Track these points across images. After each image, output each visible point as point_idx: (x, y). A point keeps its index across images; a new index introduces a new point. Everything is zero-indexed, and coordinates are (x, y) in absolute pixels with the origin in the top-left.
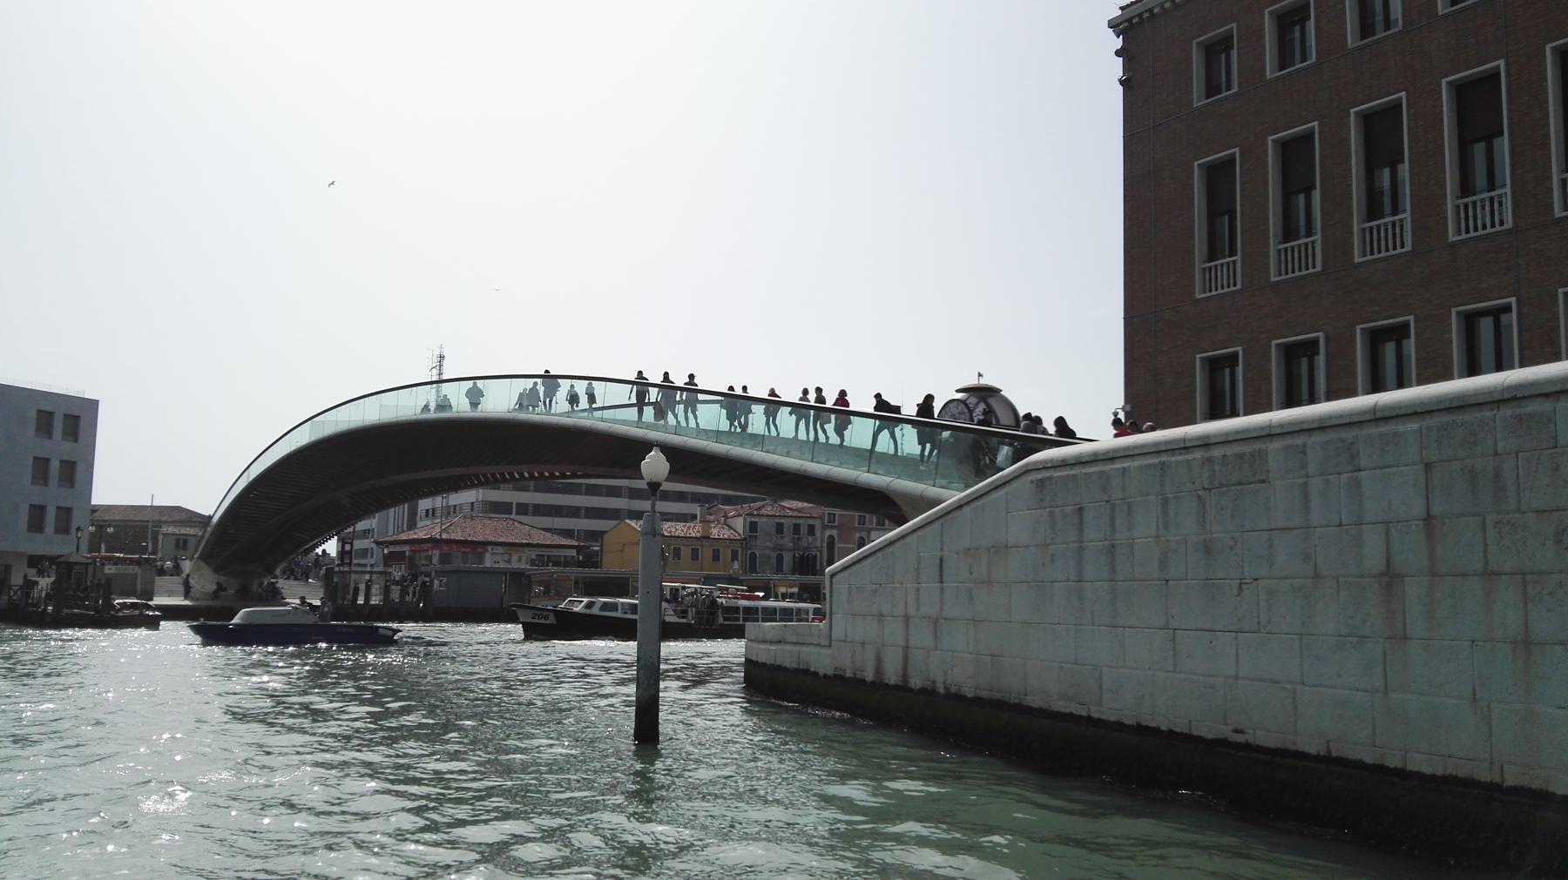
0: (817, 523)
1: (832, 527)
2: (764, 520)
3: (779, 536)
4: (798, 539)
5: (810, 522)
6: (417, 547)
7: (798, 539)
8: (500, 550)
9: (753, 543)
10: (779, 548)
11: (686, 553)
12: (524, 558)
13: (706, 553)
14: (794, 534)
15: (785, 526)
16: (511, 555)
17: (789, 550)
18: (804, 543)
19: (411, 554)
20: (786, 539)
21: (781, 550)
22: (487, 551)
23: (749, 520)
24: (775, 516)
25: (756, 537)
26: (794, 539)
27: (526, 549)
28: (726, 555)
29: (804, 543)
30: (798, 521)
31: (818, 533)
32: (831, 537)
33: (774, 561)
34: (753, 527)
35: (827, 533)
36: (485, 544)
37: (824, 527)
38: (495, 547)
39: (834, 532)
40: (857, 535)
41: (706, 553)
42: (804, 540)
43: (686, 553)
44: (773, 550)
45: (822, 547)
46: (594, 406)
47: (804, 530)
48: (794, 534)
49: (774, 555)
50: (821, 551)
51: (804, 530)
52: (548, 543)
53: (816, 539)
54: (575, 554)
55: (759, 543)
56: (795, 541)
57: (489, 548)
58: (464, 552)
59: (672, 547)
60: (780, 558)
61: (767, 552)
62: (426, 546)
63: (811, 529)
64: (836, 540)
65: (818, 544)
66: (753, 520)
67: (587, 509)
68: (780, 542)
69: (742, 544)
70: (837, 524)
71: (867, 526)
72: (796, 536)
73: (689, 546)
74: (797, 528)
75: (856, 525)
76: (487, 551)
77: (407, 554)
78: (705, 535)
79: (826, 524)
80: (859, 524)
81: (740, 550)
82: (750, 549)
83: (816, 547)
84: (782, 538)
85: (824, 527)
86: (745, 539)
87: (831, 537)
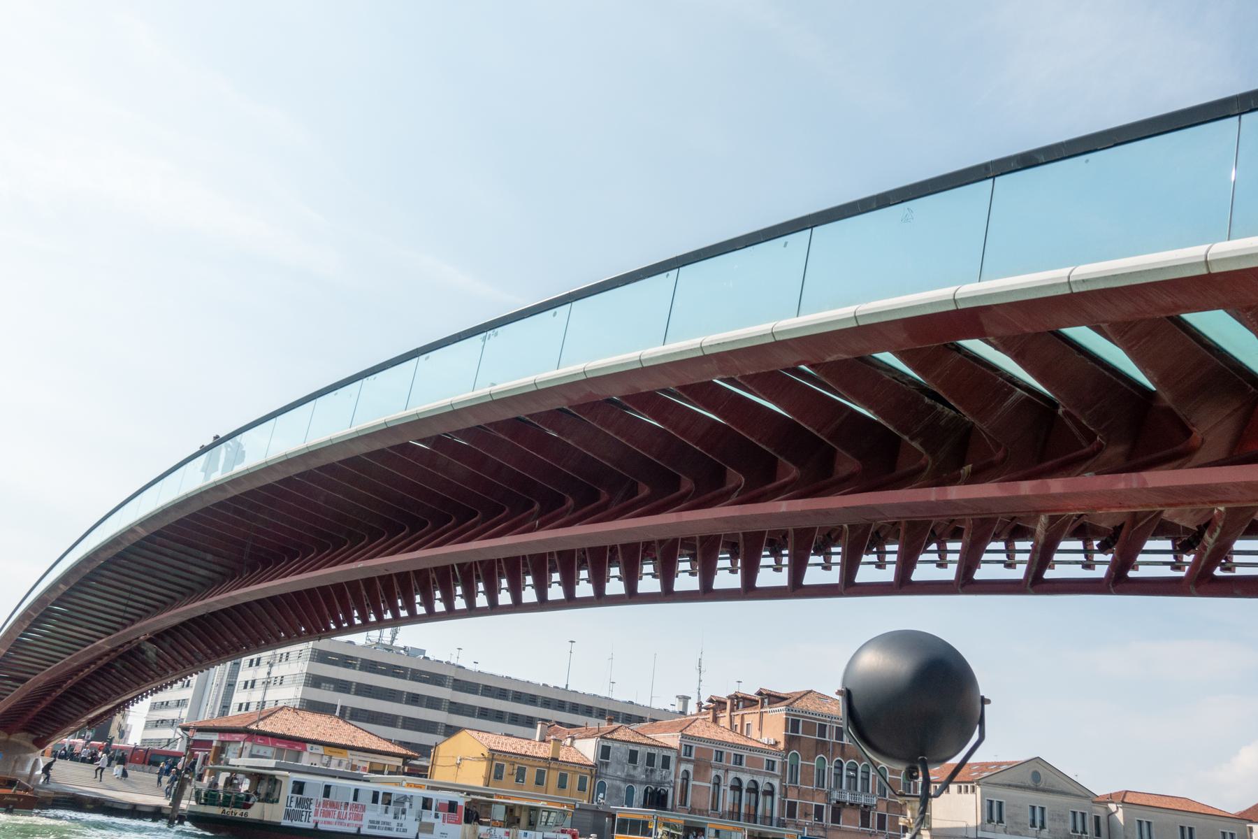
0: (673, 755)
1: (688, 761)
2: (617, 745)
3: (631, 766)
4: (652, 771)
5: (666, 753)
6: (226, 737)
8: (321, 750)
10: (630, 779)
11: (531, 774)
12: (344, 763)
13: (553, 778)
14: (647, 765)
17: (641, 783)
18: (657, 777)
19: (219, 745)
20: (639, 769)
21: (632, 782)
22: (306, 750)
23: (601, 743)
24: (629, 742)
25: (607, 764)
26: (647, 770)
27: (349, 752)
28: (573, 781)
29: (657, 777)
30: (653, 751)
31: (672, 766)
32: (687, 772)
33: (624, 795)
34: (605, 752)
35: (683, 767)
36: (304, 741)
37: (680, 760)
38: (315, 746)
39: (690, 767)
40: (714, 773)
41: (553, 778)
42: (658, 773)
43: (531, 774)
44: (625, 781)
47: (658, 762)
48: (647, 765)
49: (624, 786)
50: (674, 788)
52: (374, 748)
53: (670, 773)
54: (400, 764)
55: (610, 771)
56: (648, 773)
57: (309, 746)
58: (279, 749)
59: (516, 766)
60: (630, 791)
61: (618, 783)
62: (237, 737)
63: (666, 762)
64: (691, 777)
66: (605, 744)
67: (405, 719)
68: (632, 772)
69: (591, 770)
70: (693, 758)
71: (724, 763)
72: (650, 768)
73: (536, 767)
74: (651, 758)
76: (306, 750)
77: (214, 744)
78: (555, 757)
79: (682, 756)
80: (716, 760)
82: (600, 777)
83: (669, 783)
84: (635, 768)
85: (680, 760)
86: (595, 766)
87: (687, 772)
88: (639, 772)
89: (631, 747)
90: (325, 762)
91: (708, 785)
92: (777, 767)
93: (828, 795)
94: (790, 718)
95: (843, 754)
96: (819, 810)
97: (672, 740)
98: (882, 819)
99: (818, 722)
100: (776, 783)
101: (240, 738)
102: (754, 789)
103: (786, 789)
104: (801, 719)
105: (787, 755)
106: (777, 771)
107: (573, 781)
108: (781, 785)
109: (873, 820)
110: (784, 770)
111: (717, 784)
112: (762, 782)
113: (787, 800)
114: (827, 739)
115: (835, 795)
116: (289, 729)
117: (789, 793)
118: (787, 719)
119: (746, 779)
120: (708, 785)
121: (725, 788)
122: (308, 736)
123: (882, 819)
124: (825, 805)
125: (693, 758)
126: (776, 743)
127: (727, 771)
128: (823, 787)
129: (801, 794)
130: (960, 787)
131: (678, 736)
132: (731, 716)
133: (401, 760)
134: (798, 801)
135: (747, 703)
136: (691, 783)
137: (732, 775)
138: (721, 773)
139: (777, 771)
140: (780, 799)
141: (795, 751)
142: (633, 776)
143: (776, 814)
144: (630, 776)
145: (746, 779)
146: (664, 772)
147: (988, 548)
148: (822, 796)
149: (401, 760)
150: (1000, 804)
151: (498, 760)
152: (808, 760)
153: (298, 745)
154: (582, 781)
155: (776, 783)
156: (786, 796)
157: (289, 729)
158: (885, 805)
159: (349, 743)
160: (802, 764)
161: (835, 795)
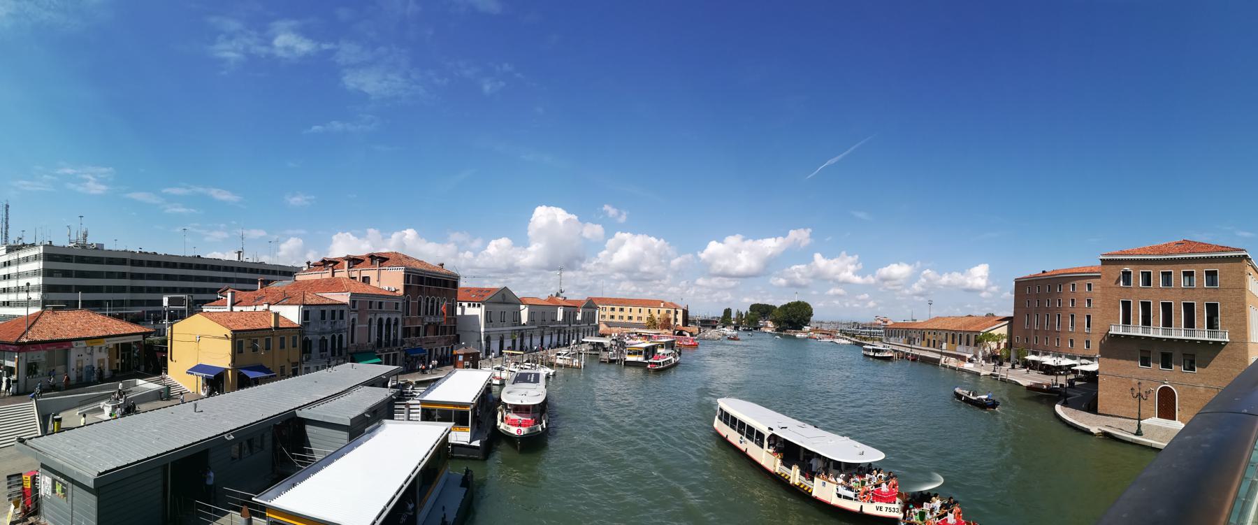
2: (313, 308)
4: (334, 322)
5: (342, 308)
7: (334, 322)
8: (84, 344)
9: (306, 329)
13: (275, 342)
15: (326, 313)
16: (92, 347)
17: (329, 333)
21: (324, 333)
27: (105, 339)
28: (288, 342)
31: (345, 317)
34: (306, 315)
39: (356, 316)
40: (369, 317)
41: (275, 342)
42: (338, 323)
44: (320, 334)
45: (348, 328)
46: (542, 330)
47: (337, 315)
50: (347, 332)
51: (337, 315)
54: (141, 339)
55: (311, 329)
65: (346, 326)
68: (324, 326)
70: (357, 309)
71: (374, 309)
73: (264, 337)
75: (368, 309)
76: (73, 347)
81: (298, 336)
83: (344, 329)
84: (325, 323)
87: (353, 320)
88: (328, 327)
89: (322, 308)
90: (89, 352)
91: (365, 326)
92: (400, 306)
93: (423, 320)
96: (418, 328)
97: (344, 298)
100: (399, 317)
101: (13, 349)
106: (400, 309)
107: (288, 342)
108: (402, 318)
110: (403, 307)
112: (393, 317)
115: (427, 319)
116: (55, 333)
118: (405, 275)
119: (385, 317)
120: (365, 326)
122: (71, 336)
125: (357, 309)
126: (396, 290)
127: (376, 315)
128: (420, 315)
129: (411, 321)
131: (347, 295)
133: (142, 336)
135: (355, 262)
136: (356, 327)
138: (372, 316)
139: (400, 309)
143: (399, 337)
144: (323, 329)
145: (385, 317)
148: (420, 322)
149: (142, 336)
151: (238, 338)
153: (65, 345)
154: (294, 339)
155: (399, 317)
156: (404, 325)
157: (55, 333)
159: (104, 334)
161: (427, 319)
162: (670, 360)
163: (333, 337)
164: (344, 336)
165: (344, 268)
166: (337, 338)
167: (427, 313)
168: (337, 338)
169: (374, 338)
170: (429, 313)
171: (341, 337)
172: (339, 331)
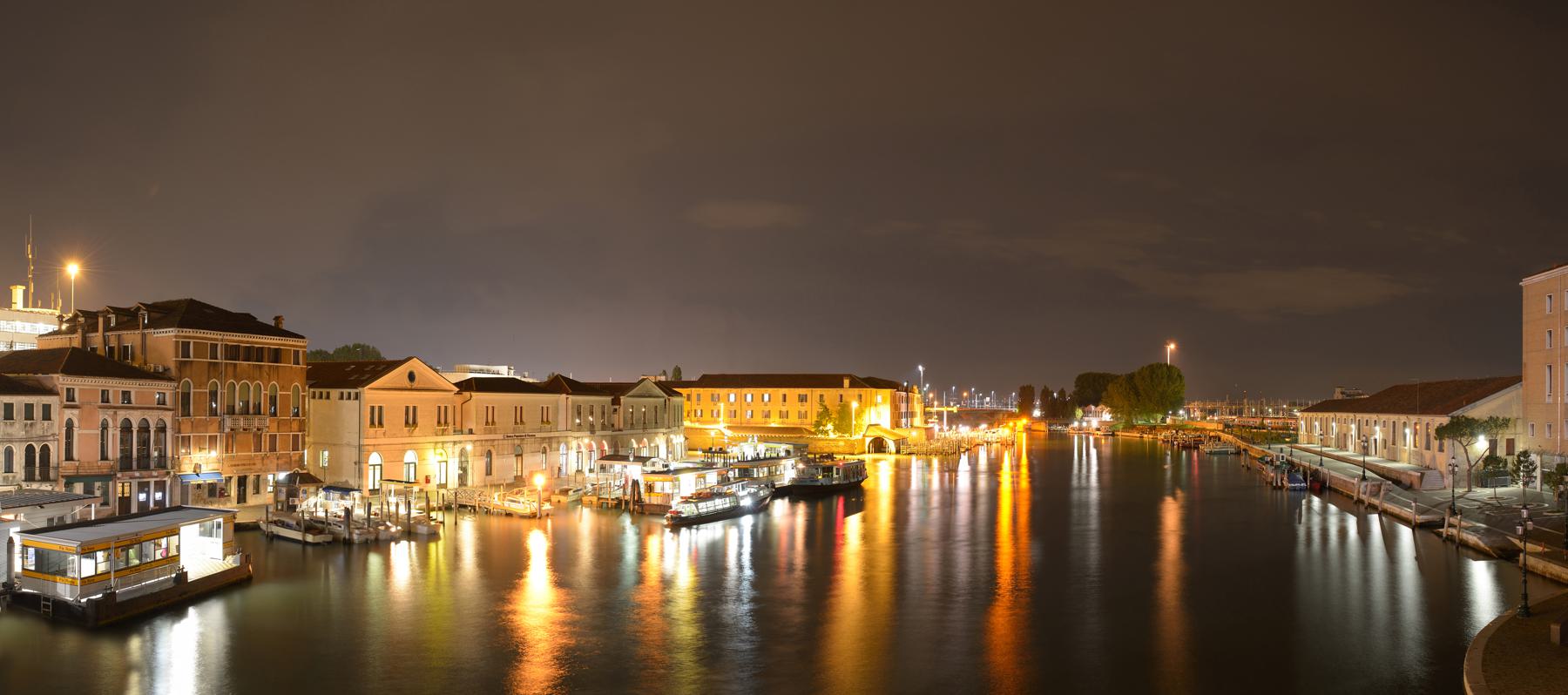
4: (31, 425)
7: (31, 425)
17: (21, 441)
20: (17, 426)
26: (26, 425)
31: (54, 415)
42: (39, 426)
56: (28, 428)
60: (9, 454)
68: (9, 430)
72: (29, 422)
83: (53, 435)
84: (12, 425)
94: (181, 340)
95: (235, 377)
98: (273, 438)
99: (209, 342)
100: (168, 417)
102: (144, 429)
103: (179, 423)
104: (192, 341)
105: (178, 386)
109: (266, 444)
111: (105, 427)
112: (153, 419)
113: (180, 435)
114: (220, 361)
117: (182, 427)
119: (135, 418)
121: (115, 432)
123: (273, 438)
124: (218, 434)
125: (77, 403)
130: (342, 393)
132: (104, 336)
134: (191, 435)
136: (76, 432)
137: (120, 418)
140: (173, 435)
141: (187, 379)
142: (11, 435)
145: (135, 418)
146: (46, 425)
147: (1333, 508)
148: (216, 425)
150: (380, 408)
152: (200, 387)
156: (179, 432)
158: (276, 424)
160: (194, 392)
162: (277, 484)
163: (30, 450)
164: (53, 447)
165: (97, 331)
166: (38, 450)
167: (372, 423)
168: (38, 450)
169: (114, 451)
170: (377, 424)
171: (45, 450)
172: (41, 438)
